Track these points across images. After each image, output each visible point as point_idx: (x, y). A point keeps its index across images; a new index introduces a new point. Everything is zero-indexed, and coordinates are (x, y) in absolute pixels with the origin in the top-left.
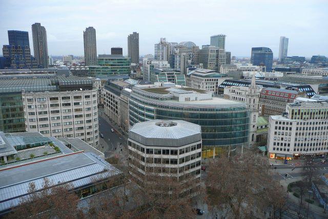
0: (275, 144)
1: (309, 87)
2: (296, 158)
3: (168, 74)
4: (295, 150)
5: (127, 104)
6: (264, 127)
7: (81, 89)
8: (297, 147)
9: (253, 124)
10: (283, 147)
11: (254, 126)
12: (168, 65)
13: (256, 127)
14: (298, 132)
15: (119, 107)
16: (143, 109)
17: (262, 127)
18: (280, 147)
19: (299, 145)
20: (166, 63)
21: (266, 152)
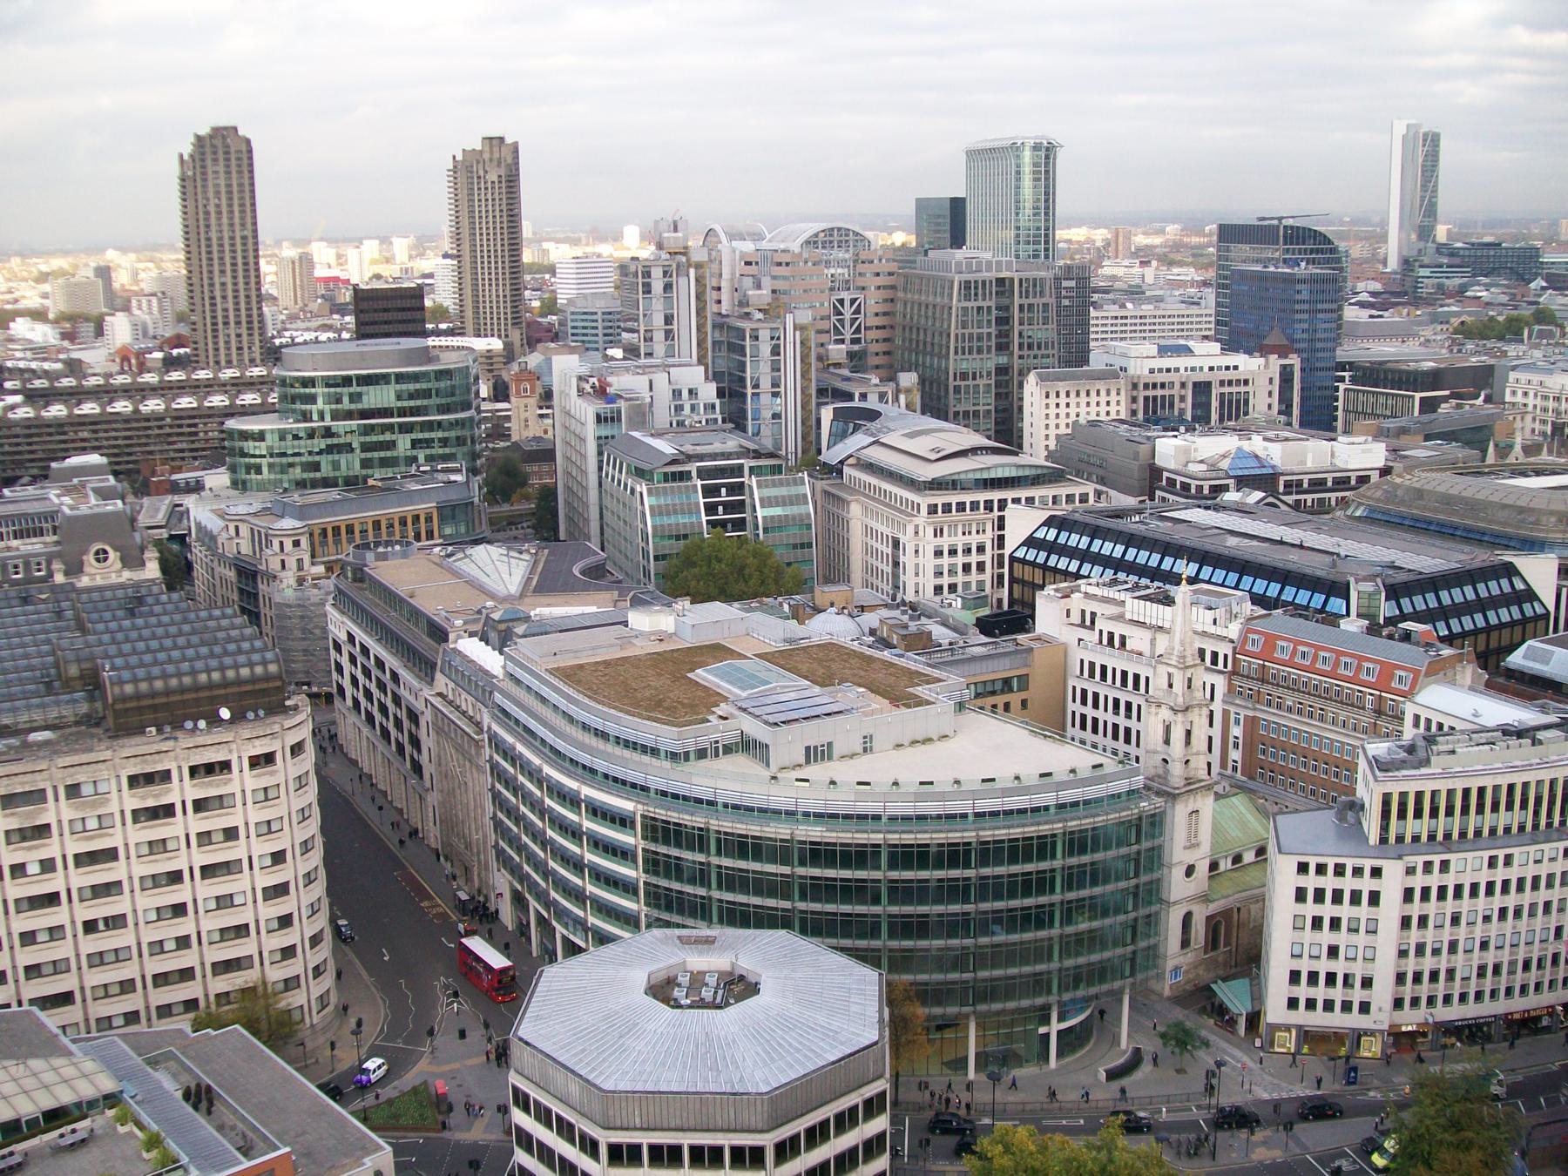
0: (1295, 977)
1: (1510, 571)
2: (1399, 1039)
3: (702, 473)
4: (1398, 1003)
5: (478, 745)
6: (1249, 857)
7: (225, 713)
8: (1408, 990)
9: (1189, 857)
10: (1337, 994)
11: (1190, 871)
12: (709, 392)
13: (1202, 869)
14: (1416, 909)
15: (427, 742)
16: (572, 800)
17: (1237, 859)
18: (1320, 992)
19: (1417, 978)
20: (693, 376)
21: (1254, 1019)
